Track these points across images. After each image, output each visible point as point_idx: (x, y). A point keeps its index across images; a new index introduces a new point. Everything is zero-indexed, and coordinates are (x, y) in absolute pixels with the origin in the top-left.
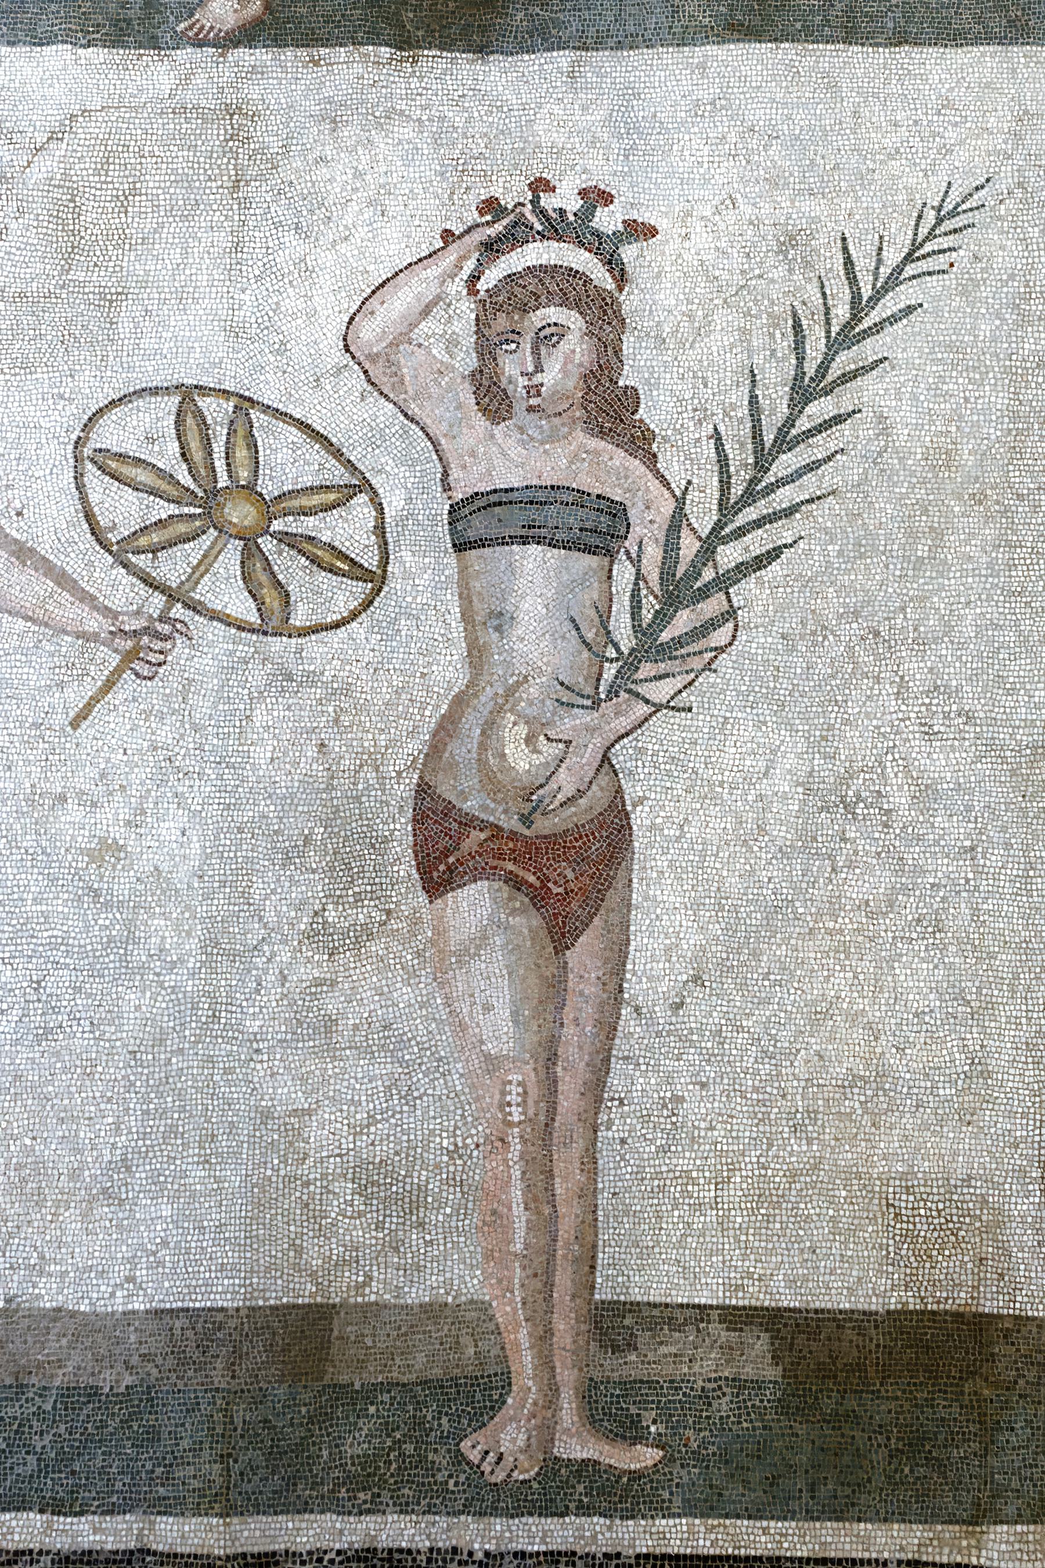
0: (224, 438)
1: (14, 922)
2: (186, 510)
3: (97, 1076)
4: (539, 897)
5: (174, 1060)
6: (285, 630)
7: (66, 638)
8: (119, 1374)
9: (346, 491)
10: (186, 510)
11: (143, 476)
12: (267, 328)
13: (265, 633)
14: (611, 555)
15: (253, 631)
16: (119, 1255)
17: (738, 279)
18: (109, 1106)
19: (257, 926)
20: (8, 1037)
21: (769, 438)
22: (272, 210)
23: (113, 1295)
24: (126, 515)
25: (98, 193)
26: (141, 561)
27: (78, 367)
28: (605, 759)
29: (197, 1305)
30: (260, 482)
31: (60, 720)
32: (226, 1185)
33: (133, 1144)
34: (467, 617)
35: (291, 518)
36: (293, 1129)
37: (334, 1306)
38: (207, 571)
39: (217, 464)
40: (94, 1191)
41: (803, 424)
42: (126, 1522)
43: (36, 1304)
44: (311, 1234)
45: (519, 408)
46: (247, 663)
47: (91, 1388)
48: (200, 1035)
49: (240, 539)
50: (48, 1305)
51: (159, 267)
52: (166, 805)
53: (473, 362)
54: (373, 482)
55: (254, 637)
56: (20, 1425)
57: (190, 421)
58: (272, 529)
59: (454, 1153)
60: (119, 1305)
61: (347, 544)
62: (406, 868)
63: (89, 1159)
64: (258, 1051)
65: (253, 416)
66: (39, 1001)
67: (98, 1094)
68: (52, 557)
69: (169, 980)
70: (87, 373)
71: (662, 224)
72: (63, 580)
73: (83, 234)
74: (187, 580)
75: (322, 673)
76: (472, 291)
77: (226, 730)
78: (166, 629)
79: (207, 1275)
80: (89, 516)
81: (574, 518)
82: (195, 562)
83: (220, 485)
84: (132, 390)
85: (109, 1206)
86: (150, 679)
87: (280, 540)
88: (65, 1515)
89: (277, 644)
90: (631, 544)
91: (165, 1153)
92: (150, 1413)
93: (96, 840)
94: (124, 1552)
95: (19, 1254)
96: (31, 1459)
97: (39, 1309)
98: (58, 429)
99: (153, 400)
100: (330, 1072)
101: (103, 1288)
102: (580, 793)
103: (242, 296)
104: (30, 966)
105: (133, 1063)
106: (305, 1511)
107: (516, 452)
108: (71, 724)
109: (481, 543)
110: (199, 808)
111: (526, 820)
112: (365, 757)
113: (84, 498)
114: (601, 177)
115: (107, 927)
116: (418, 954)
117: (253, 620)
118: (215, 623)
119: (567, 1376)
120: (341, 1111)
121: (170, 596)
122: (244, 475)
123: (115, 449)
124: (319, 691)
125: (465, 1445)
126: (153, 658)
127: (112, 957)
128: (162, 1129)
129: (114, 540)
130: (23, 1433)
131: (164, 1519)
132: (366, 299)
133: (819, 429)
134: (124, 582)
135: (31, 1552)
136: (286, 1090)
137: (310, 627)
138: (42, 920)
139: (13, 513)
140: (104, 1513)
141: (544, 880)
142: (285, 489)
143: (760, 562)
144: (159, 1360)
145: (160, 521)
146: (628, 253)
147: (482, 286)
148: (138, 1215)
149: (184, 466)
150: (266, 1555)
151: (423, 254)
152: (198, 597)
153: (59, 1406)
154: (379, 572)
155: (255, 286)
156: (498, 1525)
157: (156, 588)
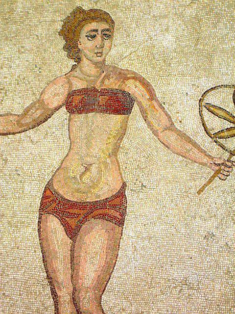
1: (178, 257)
5: (232, 309)
7: (196, 164)
20: (176, 296)
25: (207, 21)
27: (200, 76)
31: (193, 191)
66: (186, 285)
68: (191, 137)
70: (203, 78)
72: (195, 145)
78: (230, 164)
84: (218, 85)
86: (224, 180)
93: (206, 232)
104: (183, 273)
113: (202, 119)
121: (231, 153)
126: (225, 173)
129: (212, 133)
134: (216, 147)
139: (179, 121)
145: (228, 128)
157: (226, 150)
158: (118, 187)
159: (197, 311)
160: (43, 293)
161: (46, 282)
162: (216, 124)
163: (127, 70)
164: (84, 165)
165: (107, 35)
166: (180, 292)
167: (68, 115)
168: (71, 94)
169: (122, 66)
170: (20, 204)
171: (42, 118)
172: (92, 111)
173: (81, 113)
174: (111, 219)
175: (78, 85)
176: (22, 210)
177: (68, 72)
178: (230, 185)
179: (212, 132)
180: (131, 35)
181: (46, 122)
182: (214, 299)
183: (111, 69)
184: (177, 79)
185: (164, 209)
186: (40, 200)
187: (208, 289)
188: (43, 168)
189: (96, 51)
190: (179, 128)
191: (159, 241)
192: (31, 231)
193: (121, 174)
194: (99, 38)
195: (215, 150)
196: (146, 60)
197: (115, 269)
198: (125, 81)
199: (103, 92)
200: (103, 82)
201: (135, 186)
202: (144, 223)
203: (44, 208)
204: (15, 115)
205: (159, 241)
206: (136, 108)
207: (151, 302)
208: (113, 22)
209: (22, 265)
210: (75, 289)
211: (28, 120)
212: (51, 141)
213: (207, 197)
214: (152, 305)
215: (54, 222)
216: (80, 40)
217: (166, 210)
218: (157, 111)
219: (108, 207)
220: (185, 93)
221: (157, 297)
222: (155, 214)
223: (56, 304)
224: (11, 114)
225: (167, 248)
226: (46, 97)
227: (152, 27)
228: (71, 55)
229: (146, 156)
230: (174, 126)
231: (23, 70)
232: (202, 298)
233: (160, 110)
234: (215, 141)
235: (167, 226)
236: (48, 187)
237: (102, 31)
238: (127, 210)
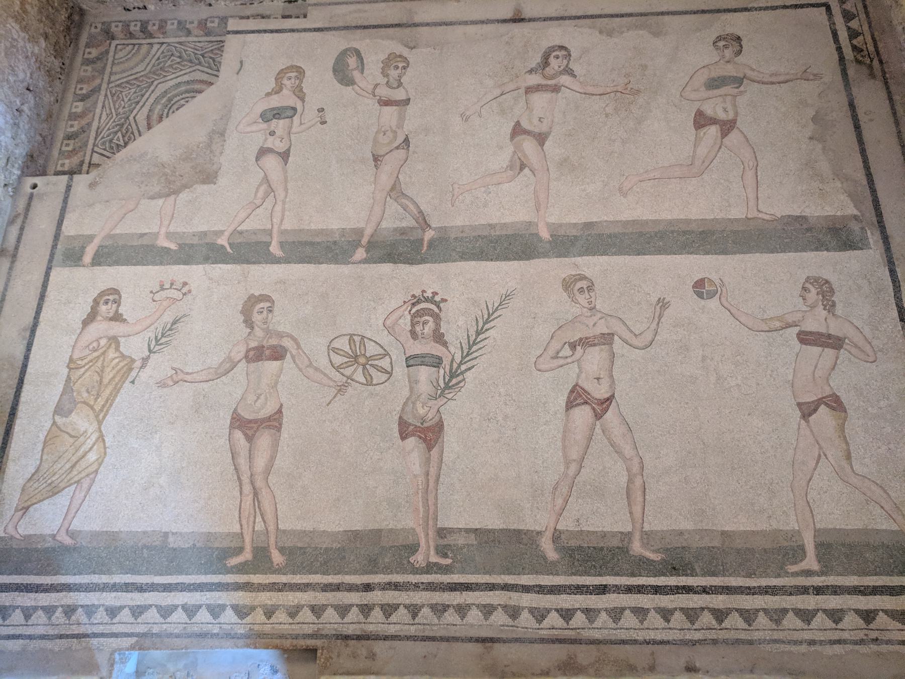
4: (425, 440)
6: (372, 384)
11: (342, 353)
14: (438, 367)
17: (464, 310)
21: (471, 343)
26: (342, 370)
28: (438, 411)
31: (324, 404)
34: (409, 381)
41: (478, 340)
45: (420, 337)
53: (410, 328)
59: (407, 496)
60: (337, 529)
62: (397, 435)
69: (348, 459)
71: (449, 299)
72: (325, 375)
76: (410, 313)
80: (331, 361)
81: (431, 360)
89: (370, 387)
90: (443, 365)
96: (319, 563)
102: (433, 418)
107: (419, 347)
109: (412, 366)
111: (422, 424)
114: (436, 290)
116: (400, 453)
119: (432, 544)
122: (363, 352)
125: (410, 559)
133: (482, 341)
141: (426, 436)
143: (469, 369)
146: (442, 305)
147: (412, 312)
156: (418, 576)
158: (278, 407)
161: (234, 472)
162: (338, 360)
168: (248, 351)
172: (262, 360)
175: (253, 344)
179: (336, 366)
192: (223, 441)
194: (265, 312)
195: (337, 377)
200: (268, 341)
206: (288, 355)
208: (274, 301)
210: (252, 475)
211: (221, 370)
226: (232, 354)
233: (303, 355)
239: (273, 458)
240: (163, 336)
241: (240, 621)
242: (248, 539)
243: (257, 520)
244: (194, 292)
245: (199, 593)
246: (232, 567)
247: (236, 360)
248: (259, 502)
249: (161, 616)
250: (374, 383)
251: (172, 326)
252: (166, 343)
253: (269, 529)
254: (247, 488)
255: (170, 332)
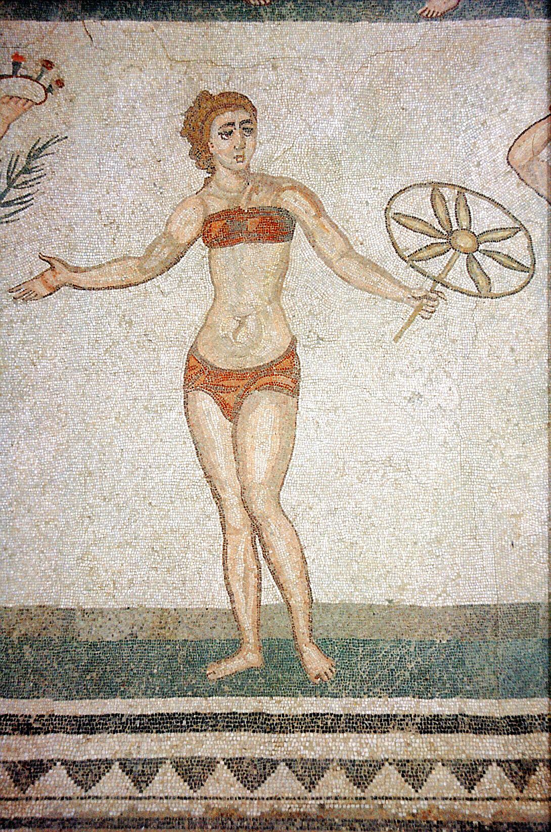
0: (454, 207)
1: (376, 431)
2: (439, 241)
3: (420, 500)
5: (455, 493)
7: (388, 300)
8: (443, 635)
9: (513, 230)
10: (439, 241)
11: (418, 226)
12: (470, 155)
13: (480, 297)
15: (475, 296)
16: (438, 581)
18: (427, 514)
19: (488, 431)
20: (378, 482)
22: (469, 99)
23: (437, 599)
24: (412, 243)
26: (419, 264)
27: (383, 175)
29: (476, 603)
30: (472, 227)
31: (388, 338)
32: (484, 549)
33: (440, 531)
35: (488, 243)
36: (513, 523)
37: (539, 604)
38: (450, 269)
39: (452, 219)
40: (424, 552)
42: (453, 702)
43: (403, 603)
44: (525, 571)
46: (473, 311)
47: (431, 641)
48: (466, 481)
49: (465, 253)
50: (408, 604)
51: (417, 127)
52: (441, 377)
54: (525, 226)
55: (476, 299)
56: (400, 658)
57: (438, 200)
58: (479, 249)
60: (440, 603)
61: (515, 255)
63: (420, 538)
64: (493, 488)
65: (466, 196)
66: (391, 466)
67: (421, 508)
68: (378, 264)
69: (449, 456)
70: (388, 177)
72: (384, 273)
73: (380, 112)
74: (442, 273)
75: (508, 315)
77: (466, 342)
79: (480, 589)
82: (445, 265)
83: (453, 229)
84: (409, 185)
85: (431, 558)
87: (484, 254)
88: (425, 698)
91: (455, 535)
92: (459, 652)
93: (410, 393)
94: (453, 715)
95: (392, 581)
96: (407, 674)
97: (403, 605)
98: (376, 204)
99: (419, 189)
100: (528, 497)
101: (432, 596)
103: (457, 140)
105: (436, 494)
106: (535, 697)
108: (394, 340)
110: (456, 378)
112: (532, 353)
113: (391, 237)
115: (418, 433)
117: (474, 291)
118: (456, 293)
120: (535, 515)
121: (435, 280)
122: (465, 224)
123: (404, 213)
124: (508, 323)
127: (422, 446)
128: (452, 524)
130: (402, 661)
131: (470, 700)
132: (516, 140)
134: (413, 274)
135: (411, 715)
136: (508, 506)
137: (501, 294)
138: (388, 430)
140: (442, 698)
142: (485, 230)
144: (461, 629)
145: (427, 246)
148: (445, 563)
149: (437, 220)
150: (519, 717)
151: (542, 118)
152: (447, 281)
153: (417, 649)
154: (532, 267)
155: (463, 135)
157: (428, 277)
159: (408, 500)
160: (202, 497)
162: (411, 241)
163: (281, 177)
164: (236, 318)
165: (248, 127)
166: (383, 476)
167: (208, 250)
168: (208, 221)
169: (273, 172)
170: (157, 381)
171: (173, 261)
172: (239, 241)
173: (225, 246)
174: (282, 387)
175: (216, 206)
176: (160, 389)
177: (200, 188)
178: (437, 324)
179: (406, 254)
180: (282, 125)
181: (178, 264)
182: (429, 481)
183: (258, 178)
184: (351, 182)
185: (351, 368)
186: (184, 373)
187: (420, 469)
188: (181, 329)
189: (235, 155)
190: (360, 253)
191: (348, 412)
192: (176, 415)
193: (288, 325)
194: (237, 133)
195: (412, 279)
196: (305, 161)
197: (294, 455)
198: (280, 193)
199: (254, 212)
201: (309, 340)
202: (326, 389)
203: (188, 381)
204: (134, 258)
205: (348, 412)
206: (299, 231)
207: (346, 495)
208: (255, 110)
209: (169, 463)
210: (243, 488)
211: (153, 263)
212: (188, 289)
213: (407, 345)
214: (348, 498)
215: (205, 401)
216: (211, 139)
217: (354, 368)
218: (328, 231)
219: (275, 373)
220: (364, 202)
221: (354, 486)
222: (339, 376)
223: (221, 508)
224: (129, 258)
225: (359, 419)
226: (174, 228)
227: (310, 111)
228: (201, 164)
229: (320, 296)
230: (354, 250)
231: (137, 192)
232: (414, 482)
233: (332, 231)
234: (411, 266)
235: (358, 391)
236: (192, 354)
237: (242, 123)
238: (302, 374)
239: (285, 454)
240: (11, 184)
241: (248, 793)
242: (247, 621)
243: (264, 584)
244: (68, 86)
245: (154, 735)
246: (220, 681)
247: (184, 240)
248: (264, 546)
249: (78, 783)
250: (496, 290)
251: (28, 163)
252: (21, 200)
253: (292, 602)
254: (236, 517)
255: (27, 177)
